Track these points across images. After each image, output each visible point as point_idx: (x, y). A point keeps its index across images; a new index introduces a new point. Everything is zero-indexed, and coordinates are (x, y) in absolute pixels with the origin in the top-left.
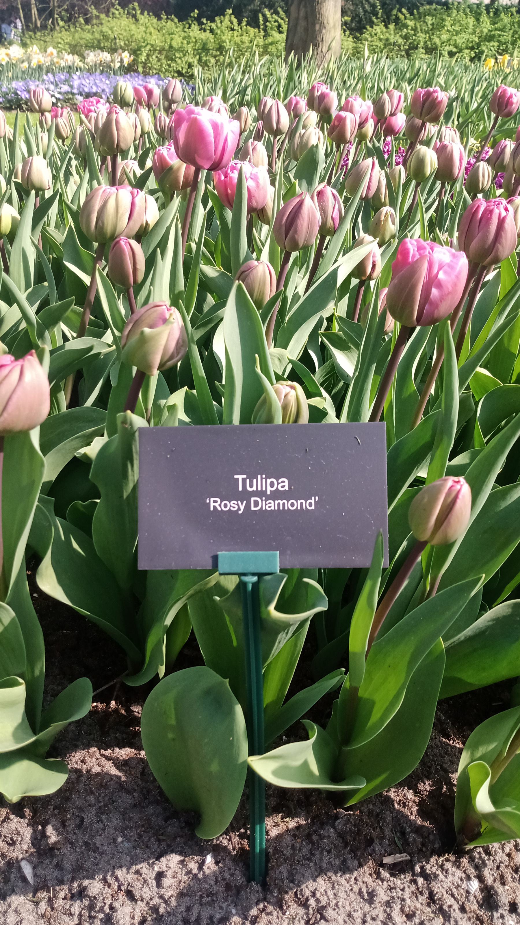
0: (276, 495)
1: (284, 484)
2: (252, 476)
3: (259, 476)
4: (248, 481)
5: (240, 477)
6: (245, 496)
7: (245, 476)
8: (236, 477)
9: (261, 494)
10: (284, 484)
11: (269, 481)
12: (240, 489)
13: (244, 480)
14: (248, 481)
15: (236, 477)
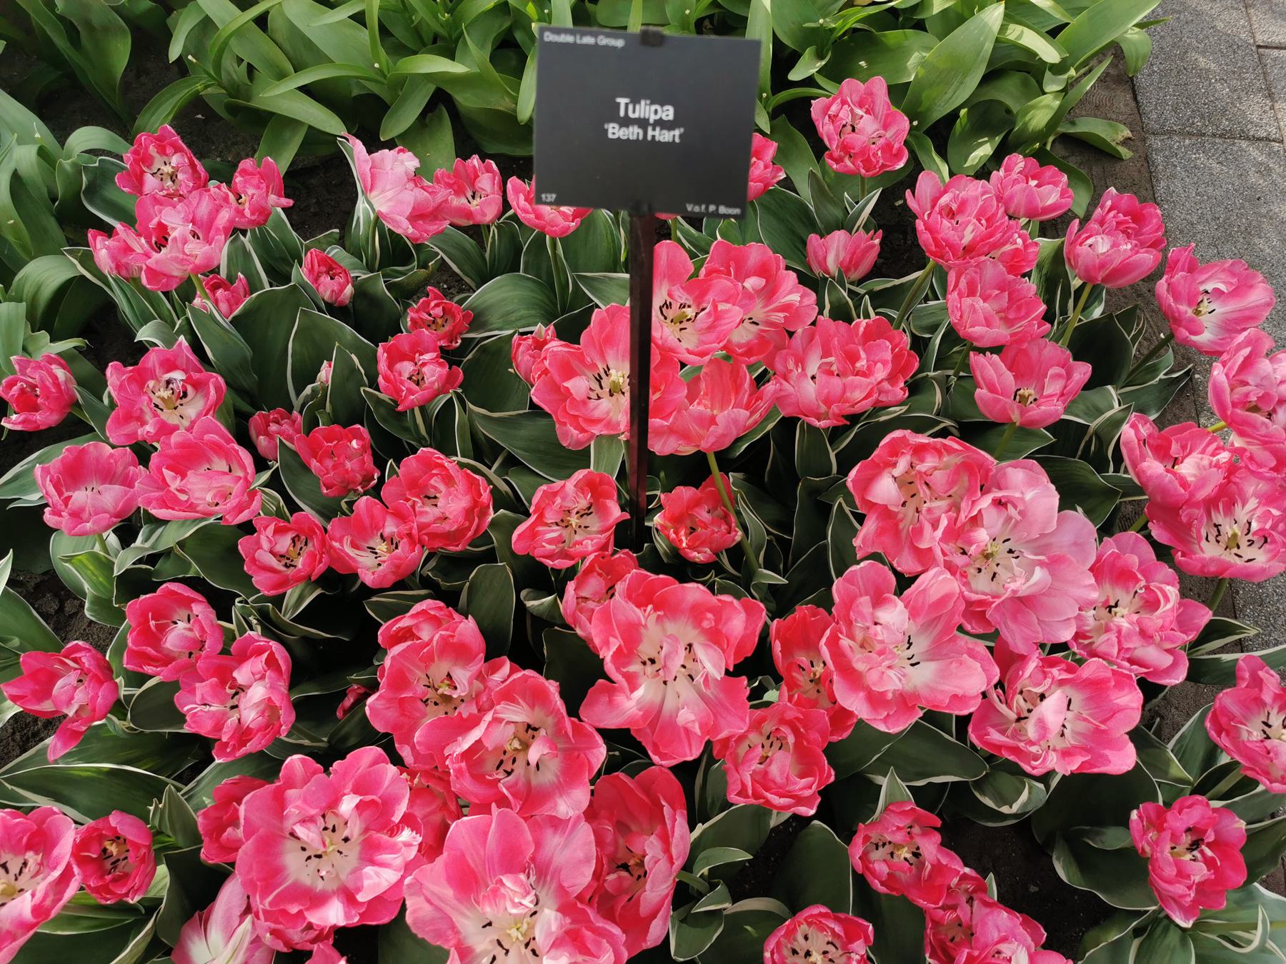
0: (661, 124)
1: (668, 113)
2: (635, 101)
3: (643, 102)
4: (631, 107)
5: (623, 101)
6: (626, 122)
7: (627, 100)
8: (619, 100)
9: (643, 123)
10: (668, 113)
11: (654, 107)
12: (622, 113)
13: (627, 105)
14: (631, 107)
15: (619, 100)
